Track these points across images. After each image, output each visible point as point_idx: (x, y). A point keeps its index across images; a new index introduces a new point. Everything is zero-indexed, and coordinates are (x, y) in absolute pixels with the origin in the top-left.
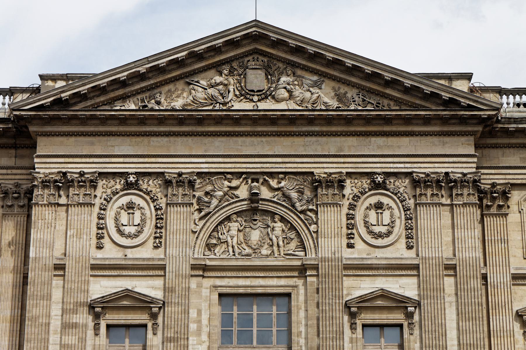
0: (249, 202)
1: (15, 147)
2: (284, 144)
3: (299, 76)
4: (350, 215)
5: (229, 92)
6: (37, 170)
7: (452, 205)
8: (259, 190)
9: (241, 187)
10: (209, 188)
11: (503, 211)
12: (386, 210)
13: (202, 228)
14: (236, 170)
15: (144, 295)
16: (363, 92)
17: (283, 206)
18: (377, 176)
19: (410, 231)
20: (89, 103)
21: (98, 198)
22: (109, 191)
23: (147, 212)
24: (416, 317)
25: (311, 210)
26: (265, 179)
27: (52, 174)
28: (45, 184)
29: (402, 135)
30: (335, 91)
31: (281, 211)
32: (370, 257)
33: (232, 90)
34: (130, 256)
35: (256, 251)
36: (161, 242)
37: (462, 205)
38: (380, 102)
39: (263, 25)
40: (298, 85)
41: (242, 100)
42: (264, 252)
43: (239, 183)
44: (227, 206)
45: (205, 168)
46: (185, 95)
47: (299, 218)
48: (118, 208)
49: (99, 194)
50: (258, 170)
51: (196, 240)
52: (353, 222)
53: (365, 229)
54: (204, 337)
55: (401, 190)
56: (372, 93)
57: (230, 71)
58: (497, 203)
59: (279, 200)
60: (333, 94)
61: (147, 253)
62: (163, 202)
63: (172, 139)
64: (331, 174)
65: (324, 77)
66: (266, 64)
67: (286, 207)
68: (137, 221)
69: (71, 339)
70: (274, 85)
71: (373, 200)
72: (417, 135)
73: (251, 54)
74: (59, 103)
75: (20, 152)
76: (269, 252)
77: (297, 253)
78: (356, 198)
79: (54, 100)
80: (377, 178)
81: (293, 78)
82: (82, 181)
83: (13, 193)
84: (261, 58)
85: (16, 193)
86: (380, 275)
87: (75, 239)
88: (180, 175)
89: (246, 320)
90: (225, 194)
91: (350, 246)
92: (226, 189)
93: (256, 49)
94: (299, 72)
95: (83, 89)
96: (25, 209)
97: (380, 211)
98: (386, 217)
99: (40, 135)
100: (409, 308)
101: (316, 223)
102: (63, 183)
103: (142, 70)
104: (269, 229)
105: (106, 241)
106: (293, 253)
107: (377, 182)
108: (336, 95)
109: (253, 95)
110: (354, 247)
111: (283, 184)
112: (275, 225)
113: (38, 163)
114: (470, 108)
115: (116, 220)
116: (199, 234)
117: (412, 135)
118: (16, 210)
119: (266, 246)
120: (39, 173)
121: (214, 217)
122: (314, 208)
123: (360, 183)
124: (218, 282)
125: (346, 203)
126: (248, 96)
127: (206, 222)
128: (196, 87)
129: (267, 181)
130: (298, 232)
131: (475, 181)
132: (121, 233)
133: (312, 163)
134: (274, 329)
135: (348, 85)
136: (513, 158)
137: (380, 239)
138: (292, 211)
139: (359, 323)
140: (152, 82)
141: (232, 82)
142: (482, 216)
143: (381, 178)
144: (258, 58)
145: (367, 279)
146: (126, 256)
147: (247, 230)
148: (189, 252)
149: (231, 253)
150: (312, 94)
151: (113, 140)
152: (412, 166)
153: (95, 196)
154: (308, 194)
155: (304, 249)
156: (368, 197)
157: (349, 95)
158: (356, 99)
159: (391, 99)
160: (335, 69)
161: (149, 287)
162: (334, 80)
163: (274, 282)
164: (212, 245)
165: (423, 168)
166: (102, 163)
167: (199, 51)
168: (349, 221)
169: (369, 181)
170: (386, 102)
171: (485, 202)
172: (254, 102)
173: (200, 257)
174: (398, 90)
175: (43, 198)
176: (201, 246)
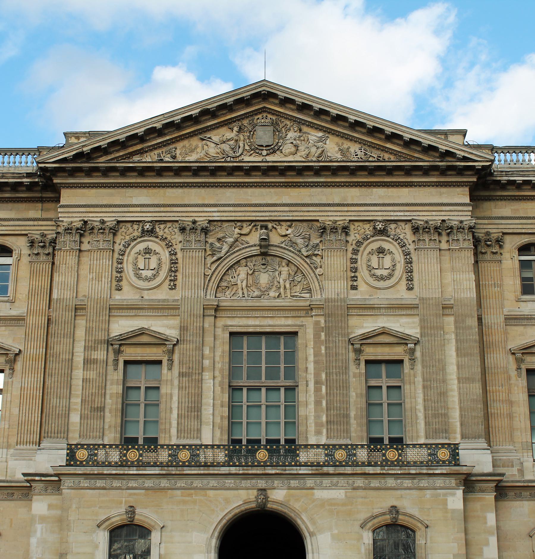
0: (258, 248)
1: (41, 200)
2: (291, 194)
3: (305, 133)
4: (353, 259)
5: (239, 147)
6: (60, 219)
7: (449, 249)
8: (268, 236)
9: (251, 235)
10: (220, 235)
11: (497, 257)
12: (388, 254)
13: (214, 271)
14: (246, 218)
15: (159, 333)
16: (364, 147)
17: (290, 251)
18: (379, 223)
19: (409, 274)
20: (109, 157)
21: (117, 244)
22: (128, 238)
23: (163, 258)
24: (418, 354)
25: (316, 255)
26: (273, 227)
27: (75, 222)
28: (68, 230)
29: (402, 186)
30: (339, 146)
31: (289, 255)
32: (372, 298)
33: (241, 145)
34: (146, 297)
35: (265, 293)
36: (176, 285)
37: (459, 249)
38: (381, 156)
39: (271, 85)
40: (304, 140)
41: (251, 154)
42: (272, 294)
43: (248, 230)
44: (237, 251)
45: (216, 216)
46: (199, 150)
47: (306, 262)
48: (136, 253)
49: (118, 241)
50: (267, 218)
51: (208, 283)
52: (355, 265)
53: (368, 272)
54: (217, 373)
55: (401, 237)
56: (374, 147)
57: (240, 128)
58: (489, 250)
59: (286, 246)
60: (337, 149)
61: (163, 294)
62: (178, 247)
63: (186, 190)
64: (336, 221)
65: (329, 133)
66: (274, 122)
67: (293, 252)
68: (153, 264)
69: (92, 375)
70: (281, 141)
71: (375, 246)
72: (415, 186)
73: (260, 113)
74: (79, 156)
75: (47, 205)
76: (278, 294)
77: (303, 295)
78: (359, 243)
79: (76, 154)
80: (378, 225)
81: (299, 134)
82: (101, 229)
83: (39, 243)
84: (270, 116)
85: (41, 242)
86: (381, 315)
87: (94, 282)
88: (194, 222)
89: (255, 357)
90: (236, 240)
91: (354, 288)
92: (236, 236)
93: (265, 107)
94: (305, 129)
95: (103, 143)
96: (50, 258)
97: (381, 255)
98: (387, 261)
99: (64, 187)
100: (409, 345)
101: (321, 267)
102: (84, 229)
103: (158, 125)
104: (277, 273)
105: (124, 283)
106: (299, 295)
107: (379, 229)
108: (340, 150)
109: (263, 150)
110: (356, 289)
111: (290, 231)
112: (283, 269)
113: (61, 212)
114: (465, 159)
115: (135, 264)
116: (211, 277)
117: (411, 186)
118: (43, 258)
119: (274, 288)
120: (62, 221)
121: (226, 262)
122: (319, 253)
123: (363, 230)
124: (229, 322)
125: (350, 249)
126: (257, 151)
127: (218, 266)
128: (208, 143)
129: (275, 228)
130: (304, 275)
131: (470, 228)
132: (139, 277)
133: (318, 211)
134: (282, 366)
135: (351, 140)
136: (505, 209)
137: (382, 281)
138: (298, 256)
139: (363, 358)
140: (168, 138)
141: (242, 138)
142: (476, 262)
143: (382, 225)
144: (267, 116)
145: (369, 318)
146: (142, 297)
147: (256, 273)
148: (202, 294)
149: (241, 295)
150: (317, 148)
151: (130, 191)
152: (412, 214)
153: (114, 242)
154: (315, 240)
155: (310, 291)
156: (370, 243)
157: (352, 150)
158: (359, 153)
159: (391, 153)
160: (339, 126)
162: (338, 136)
163: (283, 321)
164: (223, 288)
165: (422, 216)
166: (120, 212)
167: (212, 108)
168: (352, 265)
169: (371, 228)
170: (387, 156)
171: (479, 249)
172: (263, 156)
173: (212, 298)
174: (398, 145)
175: (66, 244)
176: (213, 289)
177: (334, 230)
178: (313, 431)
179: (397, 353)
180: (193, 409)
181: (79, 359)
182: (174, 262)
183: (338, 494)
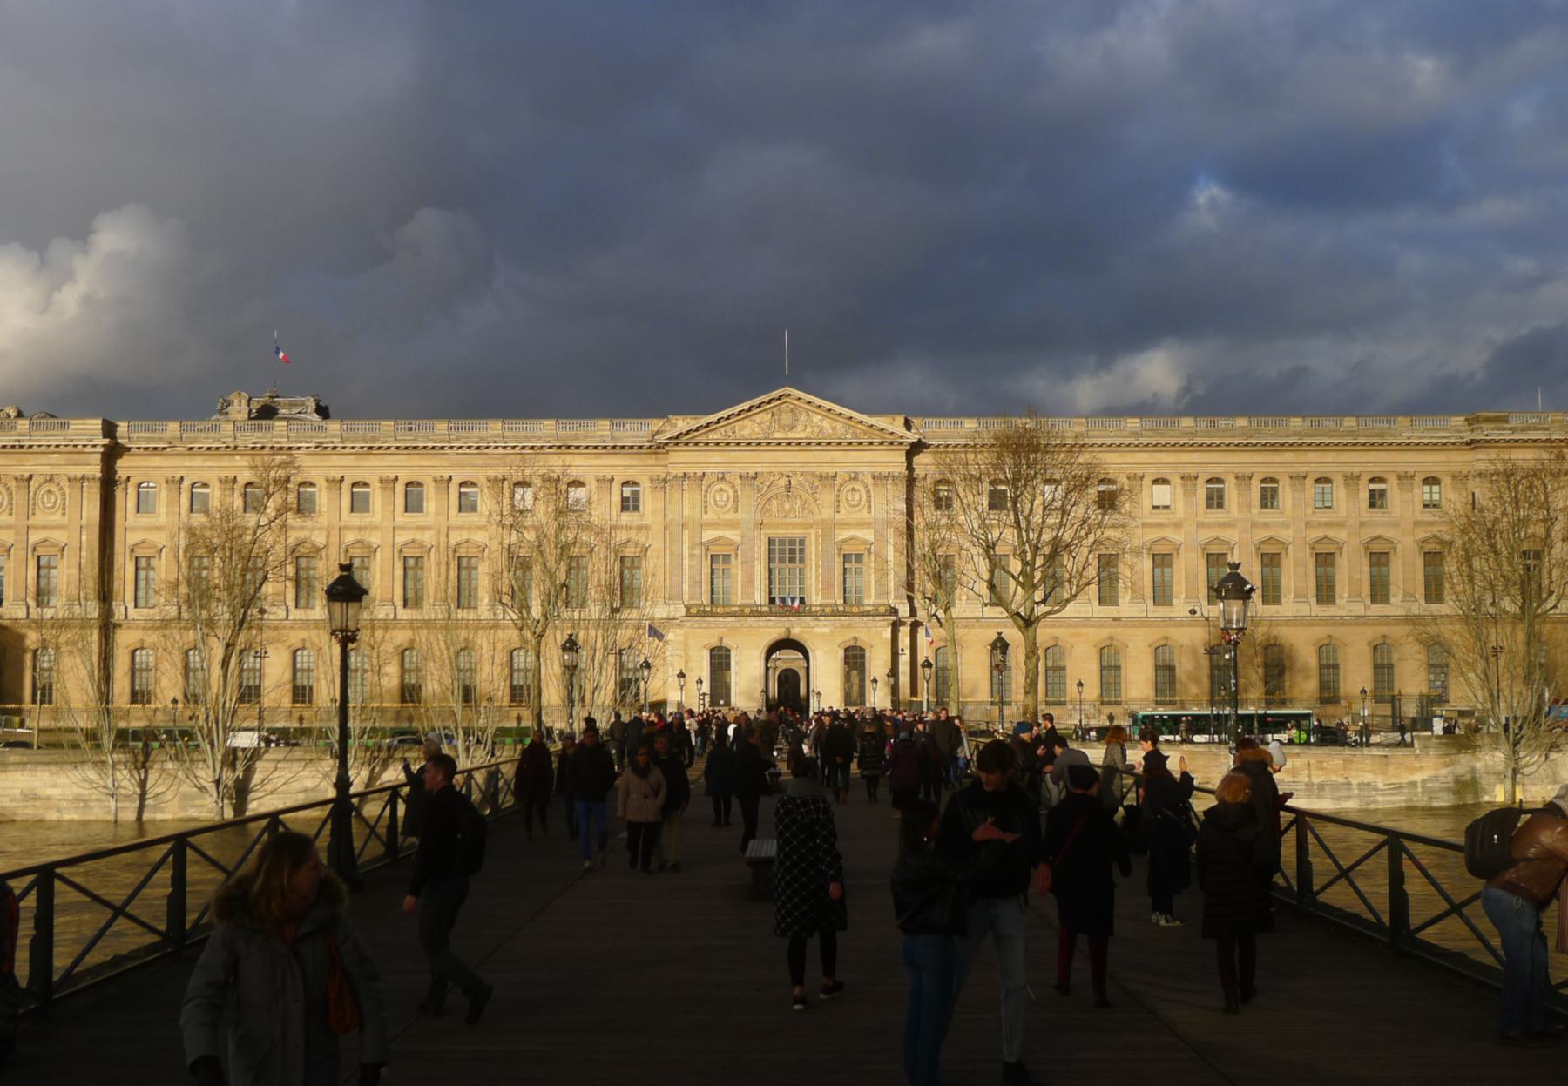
61: (730, 516)
98: (857, 497)
154: (817, 483)
161: (733, 535)
177: (827, 477)
178: (815, 599)
179: (861, 549)
180: (750, 582)
181: (686, 553)
182: (736, 497)
183: (826, 630)
